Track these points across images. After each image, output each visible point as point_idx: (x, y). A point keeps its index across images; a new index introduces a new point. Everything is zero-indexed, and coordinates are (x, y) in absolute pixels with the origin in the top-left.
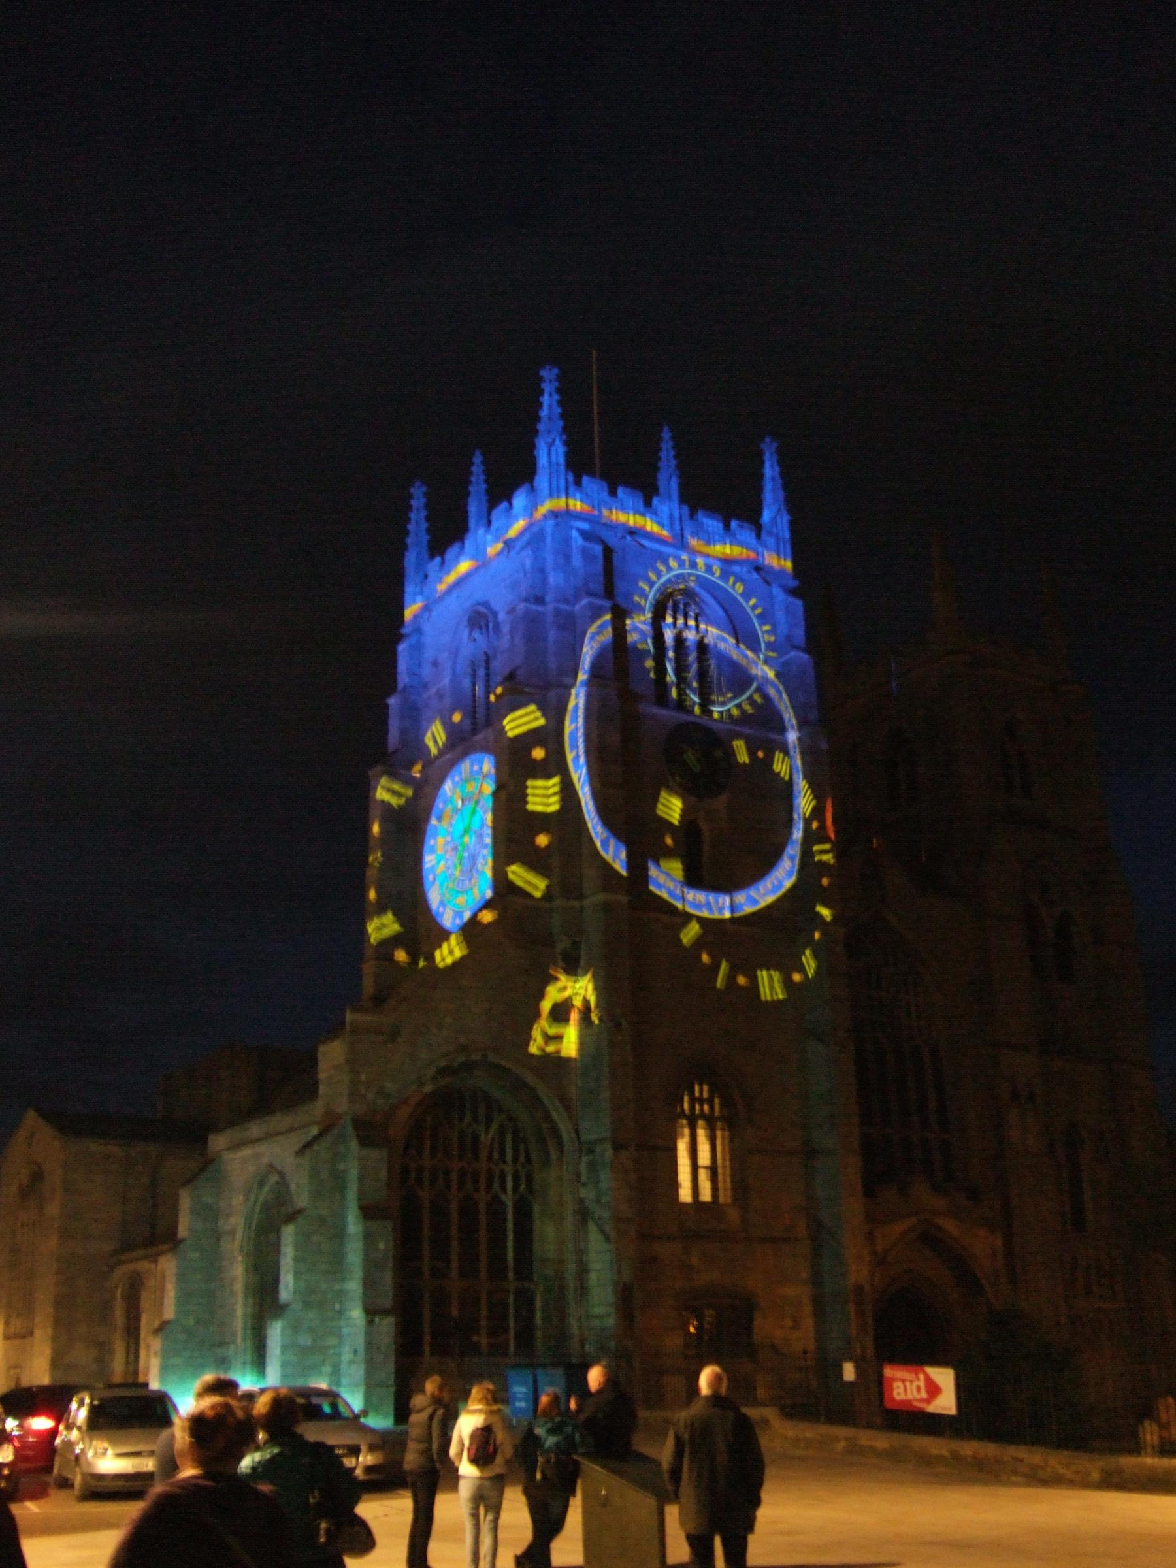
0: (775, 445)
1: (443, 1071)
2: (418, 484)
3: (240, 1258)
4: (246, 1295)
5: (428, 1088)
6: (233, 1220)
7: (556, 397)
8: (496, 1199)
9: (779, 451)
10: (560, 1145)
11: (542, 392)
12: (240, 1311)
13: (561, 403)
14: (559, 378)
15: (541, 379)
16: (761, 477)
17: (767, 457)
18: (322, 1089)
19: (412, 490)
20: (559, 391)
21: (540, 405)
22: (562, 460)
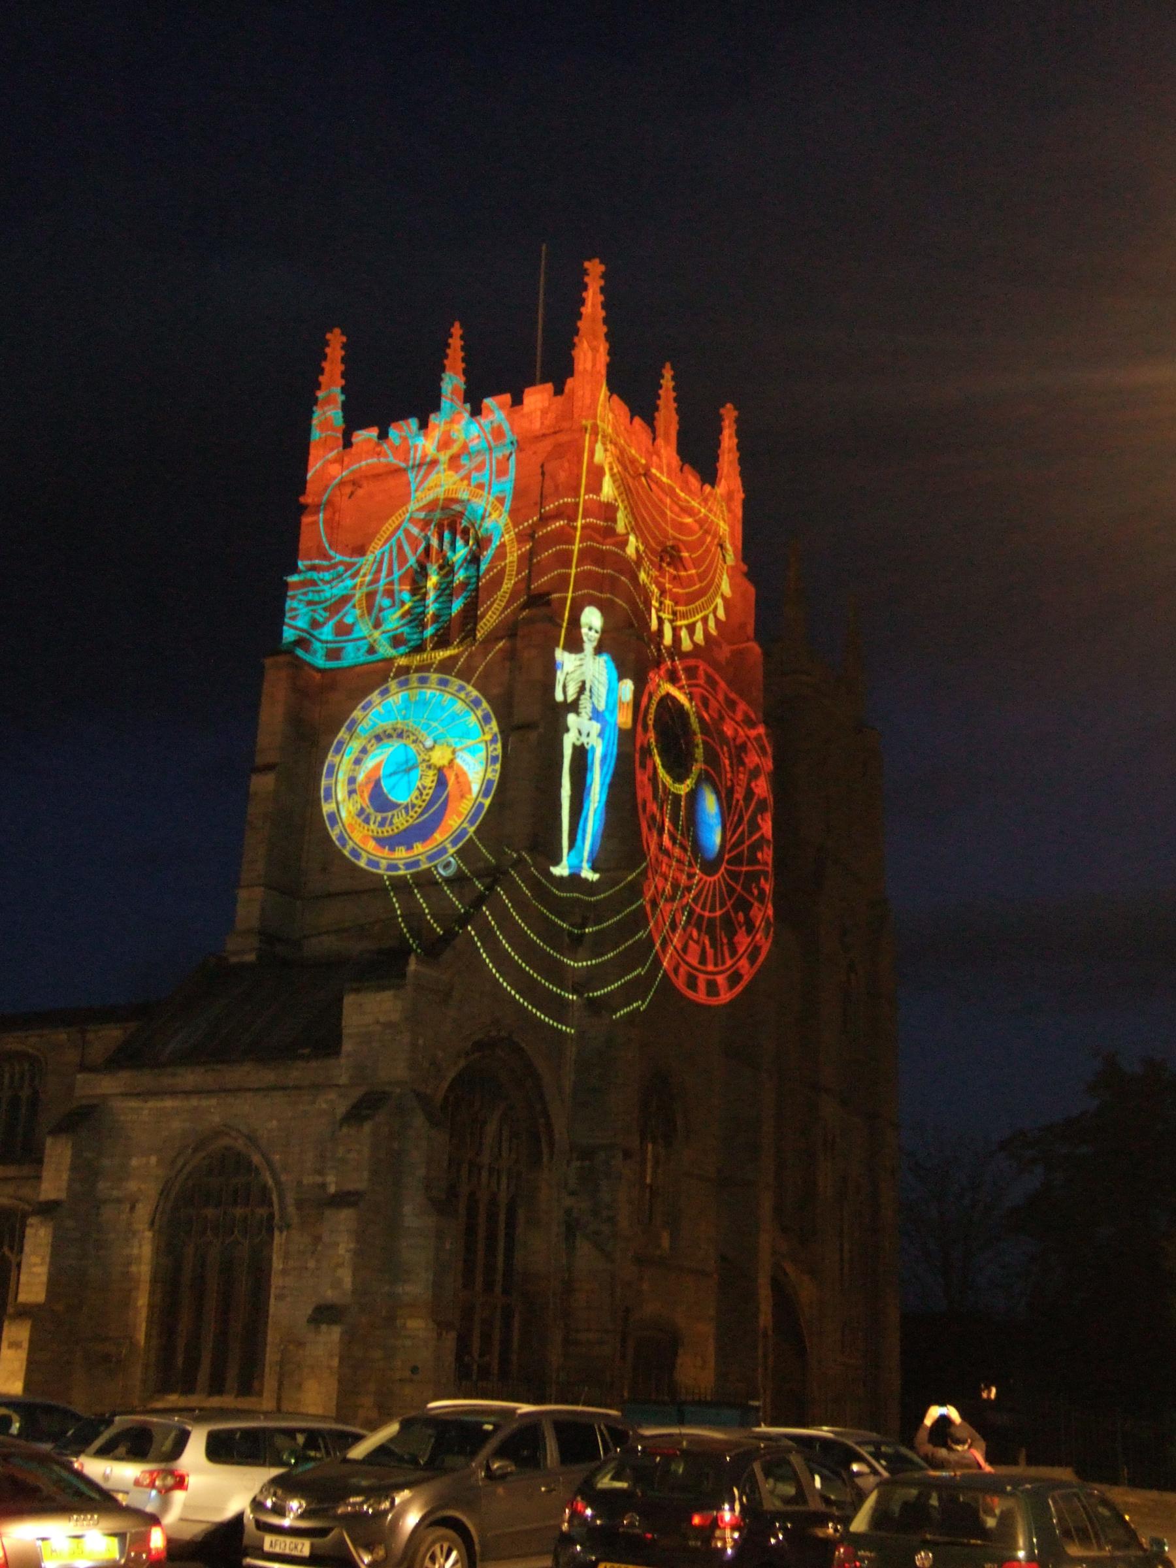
0: (736, 413)
1: (479, 1046)
2: (337, 331)
3: (149, 1234)
4: (154, 1281)
5: (462, 1063)
6: (132, 1186)
7: (601, 298)
8: (493, 1201)
9: (738, 421)
10: (551, 1145)
11: (585, 287)
12: (142, 1300)
13: (604, 306)
14: (604, 276)
15: (585, 272)
16: (718, 444)
17: (726, 423)
18: (347, 1046)
19: (329, 336)
20: (603, 290)
21: (583, 302)
22: (604, 372)
